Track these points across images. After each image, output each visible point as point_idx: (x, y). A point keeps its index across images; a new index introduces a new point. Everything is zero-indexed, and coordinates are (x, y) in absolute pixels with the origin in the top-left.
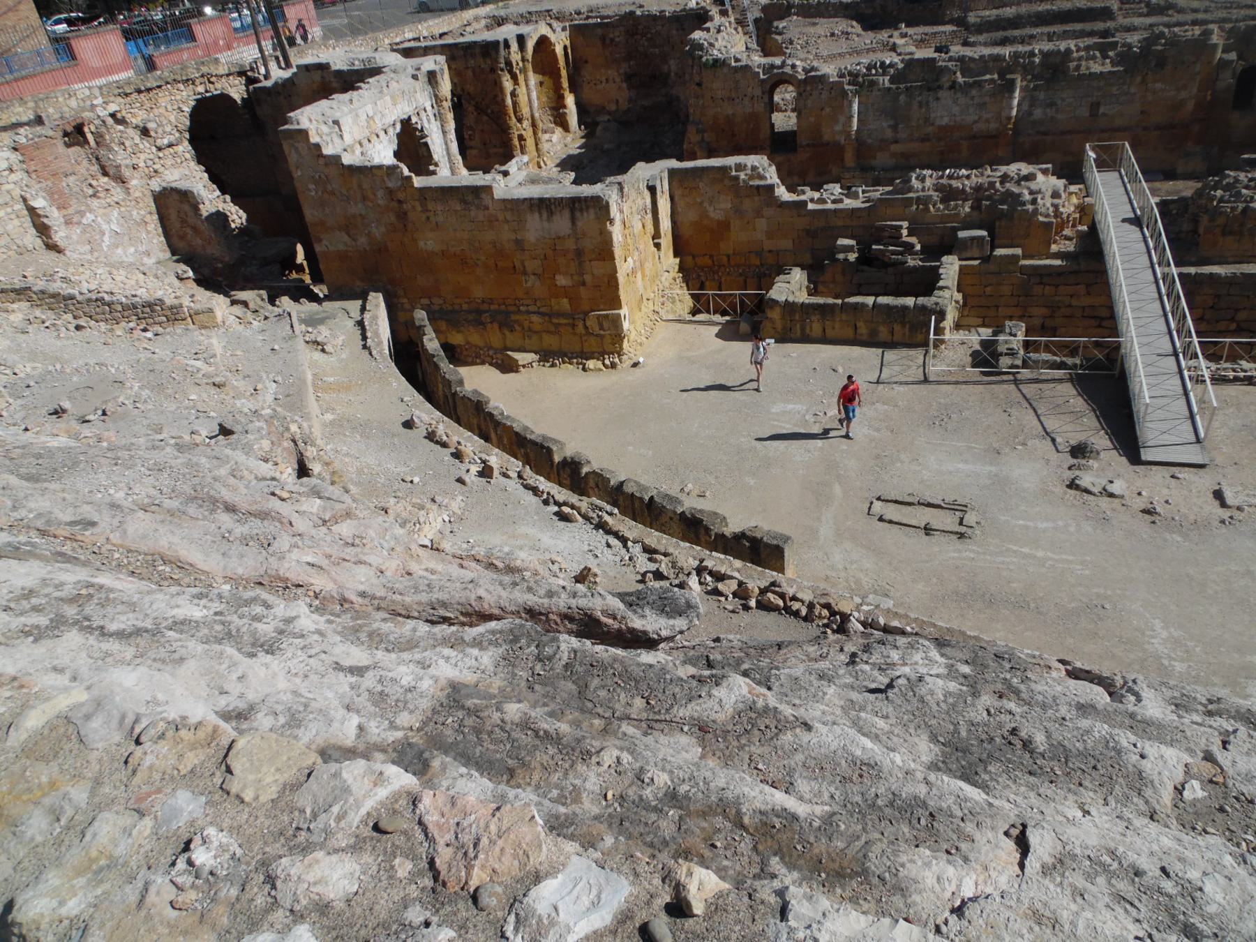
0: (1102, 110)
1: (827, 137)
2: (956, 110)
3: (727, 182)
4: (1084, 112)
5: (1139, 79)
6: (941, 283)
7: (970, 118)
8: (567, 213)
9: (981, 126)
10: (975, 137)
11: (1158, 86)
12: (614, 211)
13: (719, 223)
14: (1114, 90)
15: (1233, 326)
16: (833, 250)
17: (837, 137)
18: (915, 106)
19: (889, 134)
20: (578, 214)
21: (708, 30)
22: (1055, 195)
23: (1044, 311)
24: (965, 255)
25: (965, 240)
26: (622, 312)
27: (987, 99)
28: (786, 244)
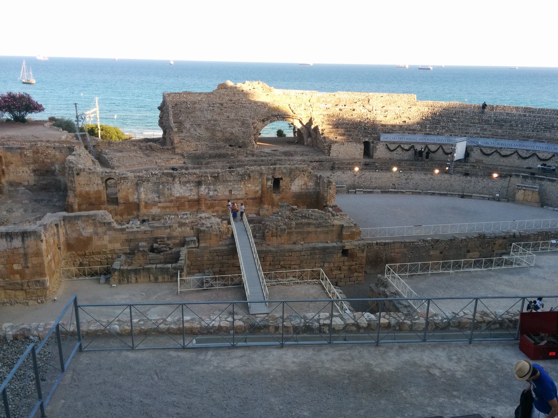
0: (233, 193)
1: (131, 200)
2: (181, 191)
3: (90, 221)
4: (227, 193)
5: (243, 183)
6: (181, 258)
7: (187, 194)
8: (20, 238)
9: (191, 197)
10: (189, 201)
11: (249, 185)
12: (43, 237)
13: (87, 238)
14: (236, 186)
15: (280, 267)
16: (137, 247)
17: (136, 200)
18: (166, 190)
19: (157, 199)
20: (26, 238)
21: (74, 155)
22: (218, 224)
23: (219, 265)
24: (189, 247)
25: (188, 242)
26: (47, 278)
27: (193, 188)
28: (117, 246)
